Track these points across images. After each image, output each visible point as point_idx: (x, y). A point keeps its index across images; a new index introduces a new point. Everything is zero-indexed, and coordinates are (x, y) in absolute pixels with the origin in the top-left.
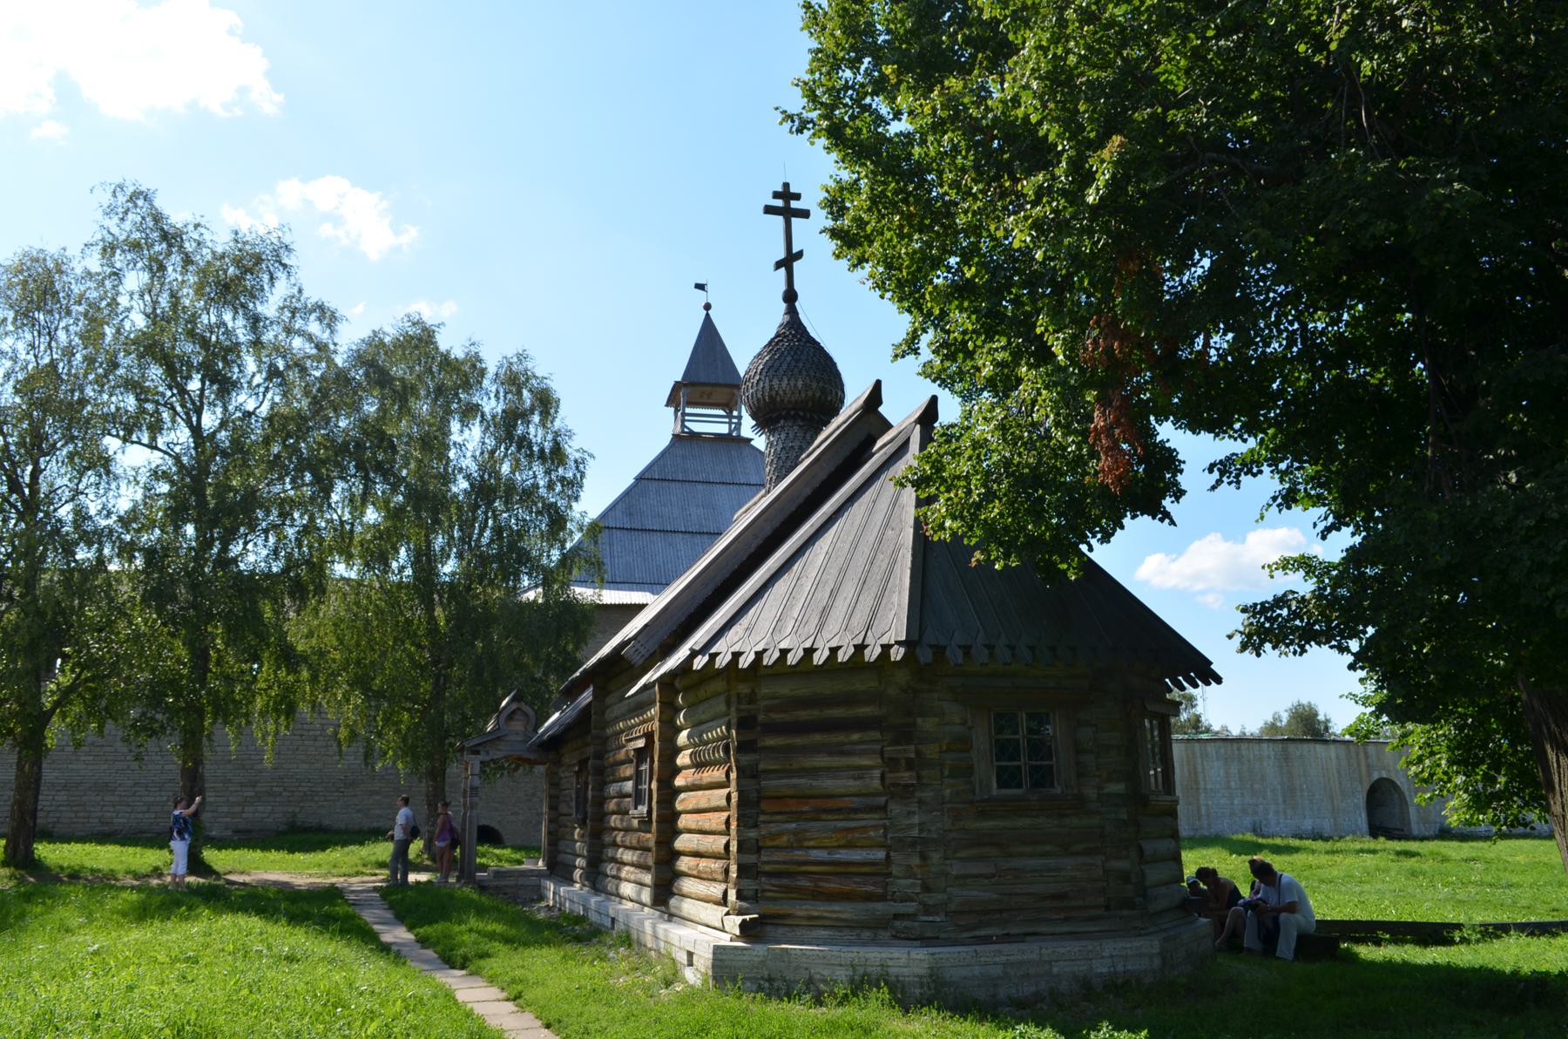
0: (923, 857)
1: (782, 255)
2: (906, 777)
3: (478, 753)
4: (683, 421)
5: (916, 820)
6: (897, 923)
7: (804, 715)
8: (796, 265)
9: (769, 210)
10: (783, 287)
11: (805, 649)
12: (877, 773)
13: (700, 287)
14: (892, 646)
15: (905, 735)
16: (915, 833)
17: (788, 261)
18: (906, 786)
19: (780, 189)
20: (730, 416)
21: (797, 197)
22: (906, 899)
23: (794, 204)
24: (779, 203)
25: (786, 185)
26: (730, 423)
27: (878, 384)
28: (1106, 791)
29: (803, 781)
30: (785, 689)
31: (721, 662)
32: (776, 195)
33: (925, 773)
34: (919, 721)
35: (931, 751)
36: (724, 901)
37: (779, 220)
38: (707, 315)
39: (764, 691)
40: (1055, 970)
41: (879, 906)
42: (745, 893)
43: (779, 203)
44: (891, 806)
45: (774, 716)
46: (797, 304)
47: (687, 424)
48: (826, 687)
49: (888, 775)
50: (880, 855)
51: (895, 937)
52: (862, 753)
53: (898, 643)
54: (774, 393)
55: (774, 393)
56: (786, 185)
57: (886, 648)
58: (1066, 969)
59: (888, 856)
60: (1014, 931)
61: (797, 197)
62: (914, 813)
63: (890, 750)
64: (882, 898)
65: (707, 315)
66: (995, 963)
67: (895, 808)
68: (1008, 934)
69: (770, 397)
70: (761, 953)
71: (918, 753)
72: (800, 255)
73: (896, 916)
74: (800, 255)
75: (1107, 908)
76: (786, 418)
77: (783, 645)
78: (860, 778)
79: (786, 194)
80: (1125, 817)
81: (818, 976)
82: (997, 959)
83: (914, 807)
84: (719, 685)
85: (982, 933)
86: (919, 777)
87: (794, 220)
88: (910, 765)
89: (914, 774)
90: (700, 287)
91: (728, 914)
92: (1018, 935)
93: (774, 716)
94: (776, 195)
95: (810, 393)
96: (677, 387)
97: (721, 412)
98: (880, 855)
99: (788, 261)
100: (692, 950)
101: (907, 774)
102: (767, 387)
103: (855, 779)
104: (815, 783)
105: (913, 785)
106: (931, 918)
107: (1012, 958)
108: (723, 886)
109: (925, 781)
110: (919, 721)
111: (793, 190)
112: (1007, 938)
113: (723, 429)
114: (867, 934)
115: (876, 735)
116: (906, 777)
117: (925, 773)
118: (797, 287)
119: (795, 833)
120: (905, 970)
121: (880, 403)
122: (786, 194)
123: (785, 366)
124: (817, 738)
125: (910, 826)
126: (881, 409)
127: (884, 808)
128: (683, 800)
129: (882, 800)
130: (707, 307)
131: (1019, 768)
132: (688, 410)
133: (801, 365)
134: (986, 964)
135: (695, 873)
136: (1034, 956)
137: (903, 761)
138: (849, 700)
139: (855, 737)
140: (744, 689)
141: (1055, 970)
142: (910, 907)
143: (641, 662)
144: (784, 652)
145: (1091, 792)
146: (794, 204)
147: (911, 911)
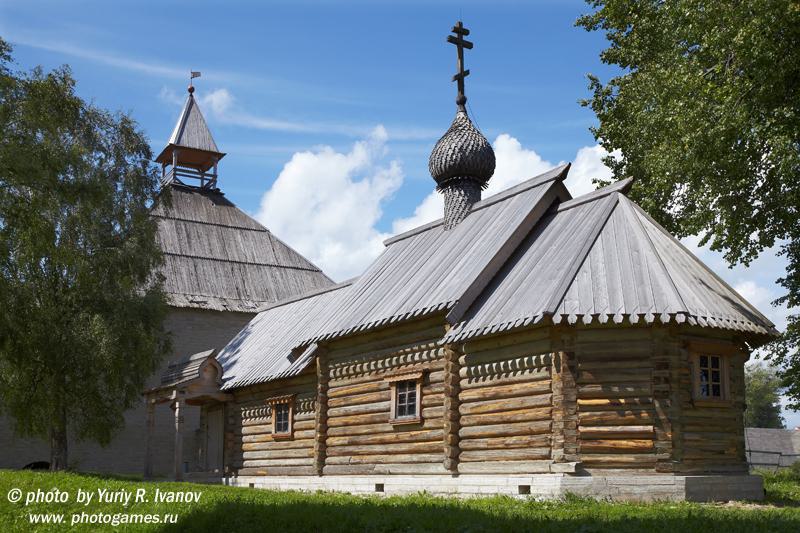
1: (457, 71)
2: (663, 386)
9: (451, 40)
14: (675, 315)
15: (665, 366)
17: (460, 78)
21: (467, 32)
22: (663, 451)
23: (465, 38)
24: (455, 35)
25: (461, 24)
30: (593, 337)
31: (572, 319)
32: (455, 30)
33: (672, 385)
35: (675, 373)
36: (548, 457)
39: (580, 338)
43: (455, 35)
46: (466, 105)
51: (658, 471)
61: (467, 32)
63: (656, 373)
72: (468, 73)
73: (660, 460)
79: (461, 31)
86: (671, 388)
88: (667, 381)
94: (455, 30)
108: (549, 449)
116: (663, 386)
118: (466, 94)
121: (565, 178)
122: (461, 31)
124: (614, 364)
131: (713, 386)
146: (465, 38)
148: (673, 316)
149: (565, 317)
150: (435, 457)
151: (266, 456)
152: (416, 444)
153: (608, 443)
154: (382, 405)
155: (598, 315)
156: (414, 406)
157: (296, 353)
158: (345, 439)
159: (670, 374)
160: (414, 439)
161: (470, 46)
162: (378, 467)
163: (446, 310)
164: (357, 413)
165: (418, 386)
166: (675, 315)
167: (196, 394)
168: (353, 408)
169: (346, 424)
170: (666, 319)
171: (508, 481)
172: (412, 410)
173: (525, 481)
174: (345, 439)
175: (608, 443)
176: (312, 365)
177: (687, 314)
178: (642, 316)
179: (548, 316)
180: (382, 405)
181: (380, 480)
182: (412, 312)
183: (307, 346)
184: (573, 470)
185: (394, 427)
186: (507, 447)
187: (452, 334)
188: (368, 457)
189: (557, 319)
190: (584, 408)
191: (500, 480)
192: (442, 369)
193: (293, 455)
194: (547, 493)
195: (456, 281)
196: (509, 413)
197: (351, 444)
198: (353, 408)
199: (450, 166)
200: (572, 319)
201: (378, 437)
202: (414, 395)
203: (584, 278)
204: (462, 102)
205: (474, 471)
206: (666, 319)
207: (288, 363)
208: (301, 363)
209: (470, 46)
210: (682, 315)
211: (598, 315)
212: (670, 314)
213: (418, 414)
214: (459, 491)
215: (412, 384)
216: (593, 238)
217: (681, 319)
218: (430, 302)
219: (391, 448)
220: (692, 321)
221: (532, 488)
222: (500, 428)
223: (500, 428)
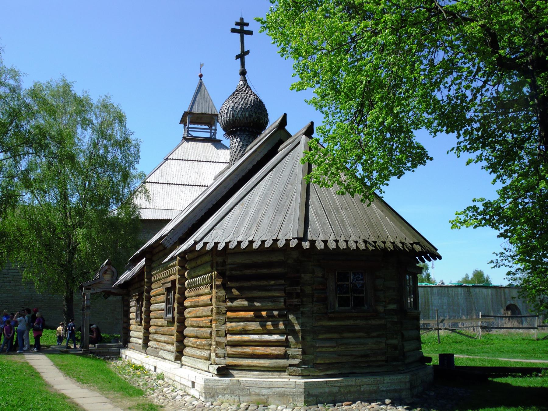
1: (239, 52)
2: (296, 301)
3: (90, 289)
4: (188, 131)
6: (291, 368)
7: (248, 272)
8: (246, 57)
9: (233, 30)
10: (239, 68)
11: (249, 241)
12: (282, 300)
17: (242, 56)
18: (296, 306)
19: (239, 21)
20: (211, 128)
21: (247, 25)
22: (294, 357)
23: (245, 28)
24: (238, 27)
25: (242, 19)
26: (211, 132)
27: (285, 115)
28: (388, 308)
30: (239, 260)
31: (209, 247)
32: (237, 24)
34: (303, 275)
35: (308, 290)
36: (209, 359)
37: (238, 36)
38: (201, 79)
39: (229, 261)
42: (220, 355)
43: (238, 27)
45: (234, 272)
47: (190, 132)
48: (258, 259)
49: (287, 301)
52: (275, 290)
53: (293, 238)
55: (234, 119)
56: (242, 19)
57: (288, 241)
61: (247, 25)
65: (201, 79)
66: (335, 386)
68: (341, 373)
69: (233, 120)
70: (227, 382)
71: (302, 290)
72: (248, 52)
73: (290, 366)
74: (248, 52)
75: (387, 361)
77: (239, 239)
78: (274, 302)
79: (242, 23)
80: (396, 320)
81: (253, 393)
84: (208, 258)
86: (302, 302)
87: (246, 36)
88: (298, 296)
89: (299, 300)
91: (211, 364)
92: (346, 373)
93: (234, 272)
94: (237, 24)
95: (252, 119)
96: (185, 114)
97: (207, 127)
99: (242, 56)
100: (194, 381)
101: (297, 300)
102: (231, 116)
103: (272, 302)
105: (299, 305)
107: (343, 384)
108: (209, 352)
110: (303, 275)
111: (245, 21)
113: (208, 135)
115: (283, 282)
116: (296, 301)
117: (305, 299)
118: (246, 68)
121: (286, 124)
122: (242, 23)
124: (254, 283)
126: (286, 128)
128: (189, 313)
130: (201, 76)
131: (348, 297)
132: (191, 126)
135: (195, 346)
136: (353, 383)
138: (270, 265)
139: (272, 282)
140: (220, 259)
141: (362, 389)
143: (170, 246)
144: (239, 243)
145: (381, 309)
146: (245, 28)
153: (247, 350)
155: (219, 243)
159: (302, 290)
161: (250, 33)
162: (162, 353)
175: (247, 350)
190: (232, 320)
204: (201, 76)
209: (250, 33)
211: (219, 243)
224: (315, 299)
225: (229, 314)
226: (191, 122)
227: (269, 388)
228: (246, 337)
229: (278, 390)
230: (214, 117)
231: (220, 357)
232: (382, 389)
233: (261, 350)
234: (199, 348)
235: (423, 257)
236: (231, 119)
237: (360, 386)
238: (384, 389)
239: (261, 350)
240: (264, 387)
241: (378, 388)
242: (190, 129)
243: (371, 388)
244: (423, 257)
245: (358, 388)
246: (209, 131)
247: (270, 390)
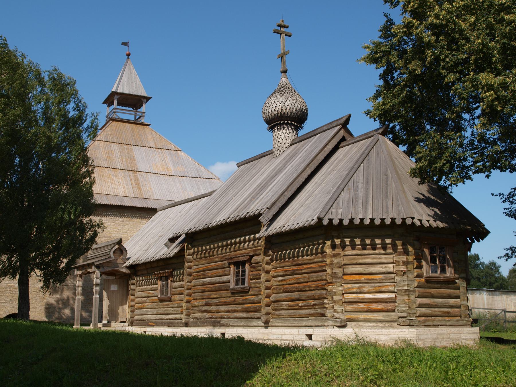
0: (409, 297)
5: (406, 283)
6: (400, 319)
13: (125, 44)
14: (406, 219)
16: (406, 288)
26: (135, 117)
29: (361, 269)
31: (336, 222)
36: (323, 315)
40: (451, 337)
41: (393, 314)
44: (396, 278)
50: (393, 296)
54: (283, 113)
57: (404, 220)
58: (454, 337)
59: (396, 296)
60: (435, 324)
62: (405, 281)
64: (393, 311)
67: (398, 279)
69: (281, 114)
70: (350, 331)
71: (407, 258)
73: (400, 317)
76: (287, 124)
78: (384, 268)
82: (435, 332)
83: (405, 278)
85: (427, 324)
90: (125, 44)
97: (131, 109)
98: (393, 296)
101: (403, 267)
102: (280, 110)
104: (366, 269)
106: (411, 318)
107: (439, 332)
109: (409, 269)
112: (434, 326)
113: (132, 118)
114: (387, 324)
116: (403, 268)
117: (409, 266)
119: (359, 288)
120: (407, 335)
121: (348, 124)
123: (288, 101)
125: (404, 286)
126: (347, 126)
127: (394, 279)
129: (393, 275)
133: (295, 102)
134: (432, 334)
137: (401, 262)
141: (451, 337)
142: (405, 314)
147: (405, 315)
148: (404, 220)
149: (331, 220)
150: (257, 315)
151: (155, 313)
152: (246, 305)
153: (363, 306)
154: (225, 278)
155: (353, 219)
156: (245, 279)
157: (172, 240)
158: (203, 302)
160: (244, 302)
162: (223, 321)
163: (260, 215)
164: (210, 283)
165: (247, 265)
166: (406, 219)
167: (108, 269)
168: (208, 280)
169: (204, 291)
170: (399, 222)
171: (298, 332)
172: (243, 283)
173: (309, 331)
174: (203, 302)
176: (182, 250)
177: (413, 218)
178: (383, 220)
179: (320, 220)
180: (225, 278)
181: (223, 330)
182: (240, 215)
183: (180, 236)
184: (338, 325)
185: (232, 293)
186: (301, 308)
187: (263, 233)
188: (216, 314)
189: (325, 222)
191: (295, 331)
192: (260, 254)
193: (171, 312)
194: (322, 340)
195: (270, 194)
196: (301, 285)
197: (206, 305)
198: (208, 280)
199: (274, 115)
200: (336, 222)
201: (223, 300)
202: (244, 272)
203: (345, 195)
205: (281, 324)
206: (399, 222)
207: (166, 248)
208: (174, 249)
210: (411, 219)
211: (353, 219)
212: (402, 219)
213: (246, 285)
214: (271, 338)
215: (243, 263)
216: (356, 166)
217: (409, 222)
218: (252, 209)
219: (230, 308)
220: (418, 223)
221: (313, 336)
222: (296, 295)
223: (296, 295)
224: (415, 267)
225: (345, 277)
226: (118, 104)
227: (387, 335)
228: (361, 296)
229: (393, 336)
230: (142, 99)
231: (338, 313)
232: (463, 338)
233: (374, 306)
234: (304, 309)
235: (468, 238)
236: (279, 113)
237: (449, 334)
238: (464, 338)
239: (374, 306)
240: (382, 335)
241: (460, 337)
242: (117, 111)
243: (456, 337)
244: (468, 238)
245: (449, 336)
246: (134, 113)
247: (387, 337)
